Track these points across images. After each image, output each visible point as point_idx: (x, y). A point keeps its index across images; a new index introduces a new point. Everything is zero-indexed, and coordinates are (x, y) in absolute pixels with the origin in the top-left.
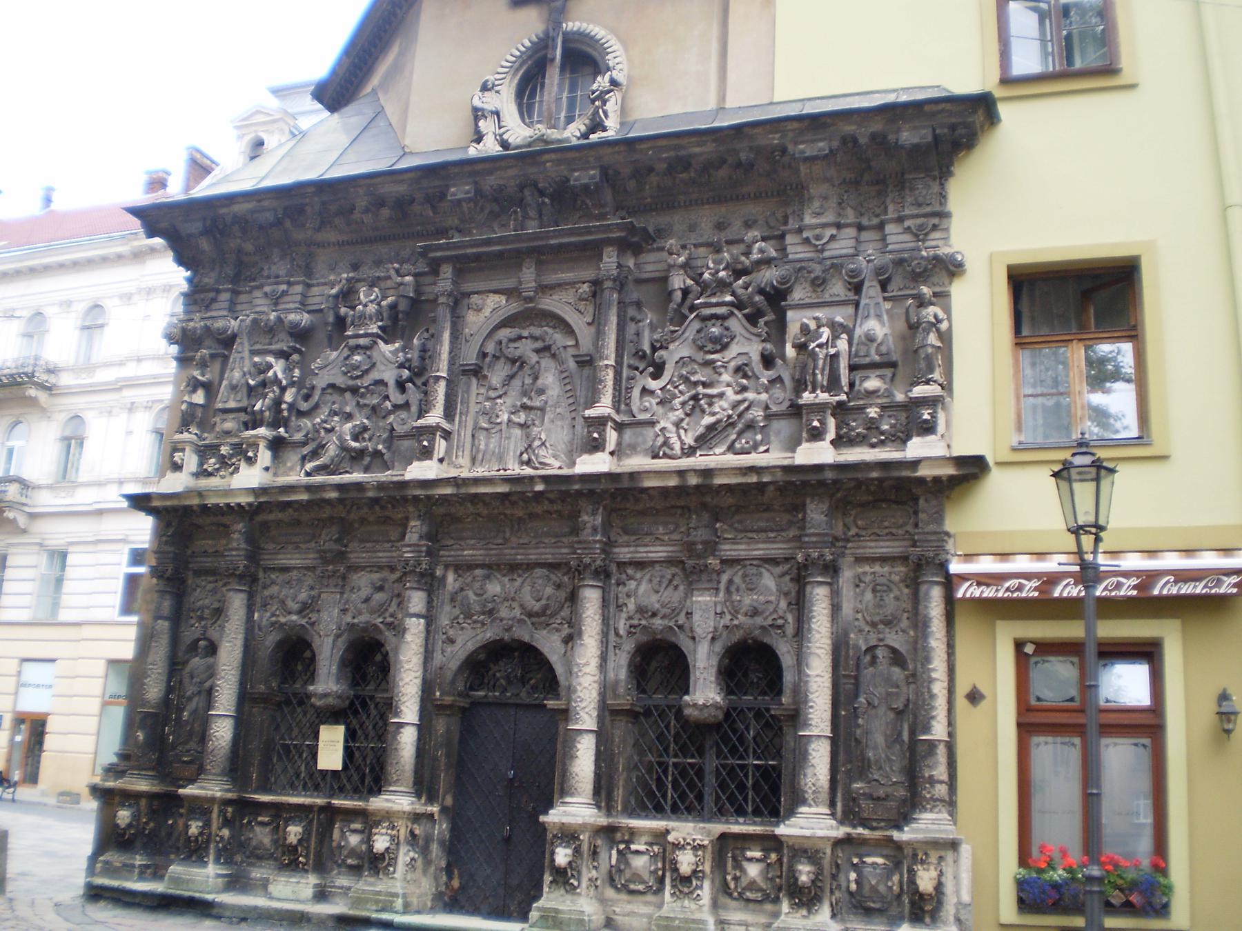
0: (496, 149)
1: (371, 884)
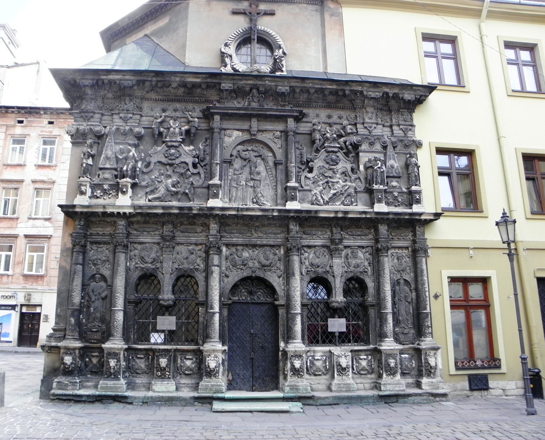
0: (232, 72)
1: (208, 382)
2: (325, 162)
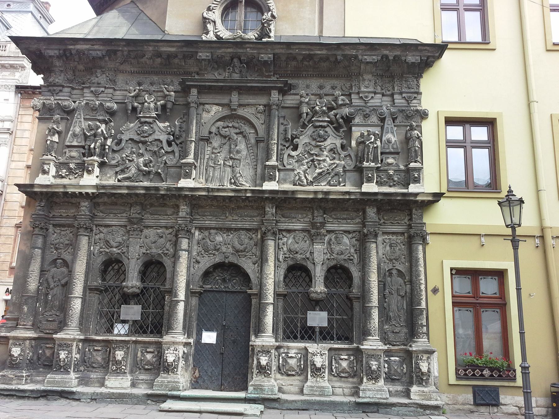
1: (164, 378)
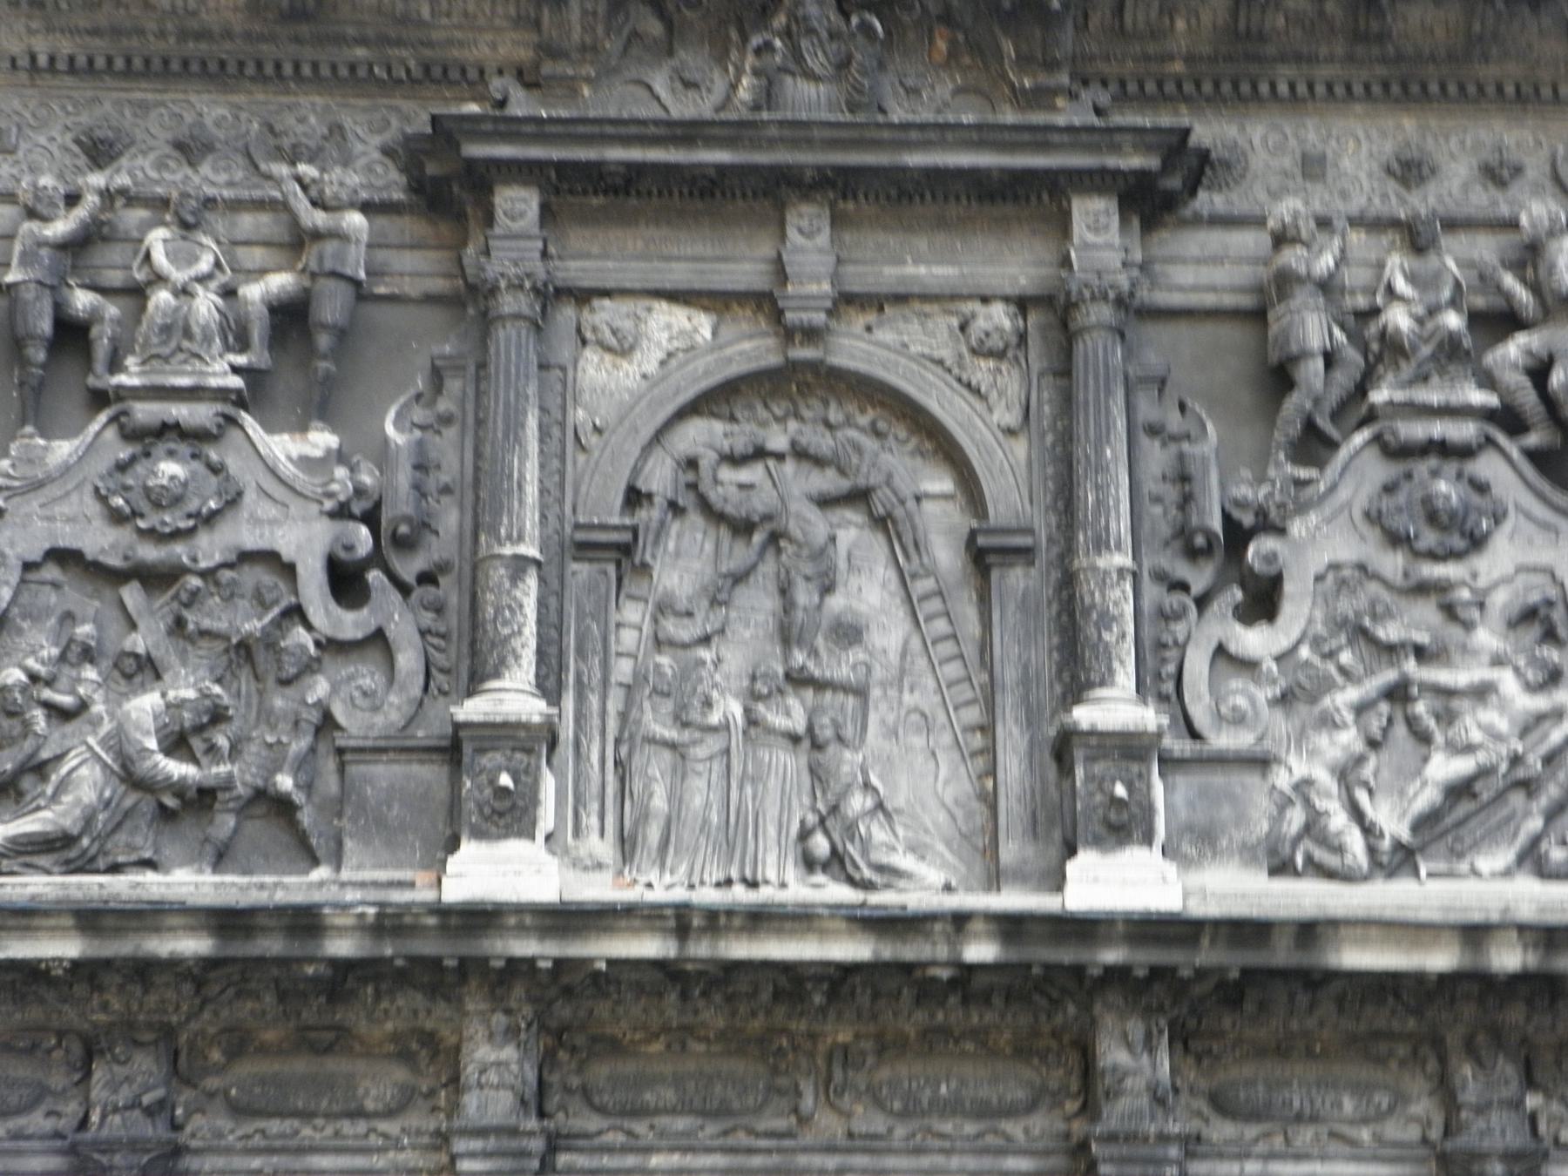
2: (1373, 534)
